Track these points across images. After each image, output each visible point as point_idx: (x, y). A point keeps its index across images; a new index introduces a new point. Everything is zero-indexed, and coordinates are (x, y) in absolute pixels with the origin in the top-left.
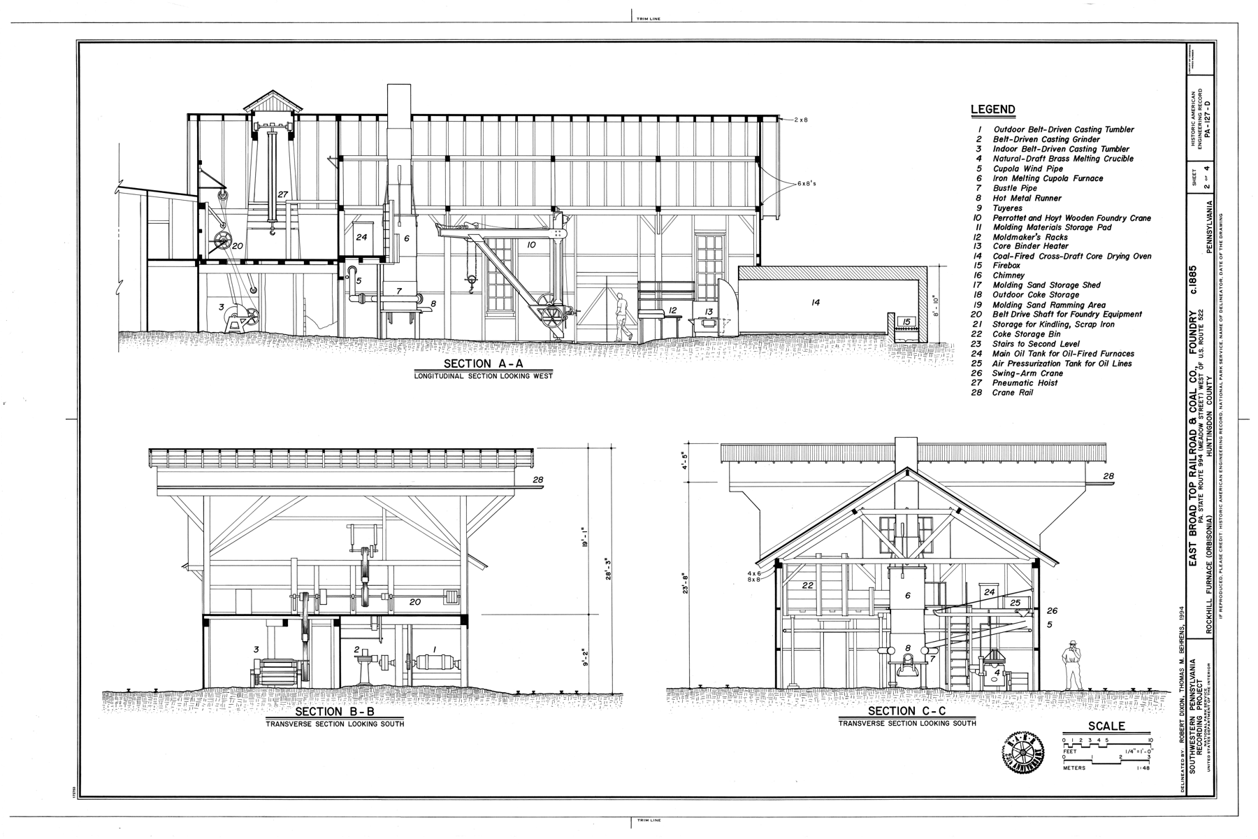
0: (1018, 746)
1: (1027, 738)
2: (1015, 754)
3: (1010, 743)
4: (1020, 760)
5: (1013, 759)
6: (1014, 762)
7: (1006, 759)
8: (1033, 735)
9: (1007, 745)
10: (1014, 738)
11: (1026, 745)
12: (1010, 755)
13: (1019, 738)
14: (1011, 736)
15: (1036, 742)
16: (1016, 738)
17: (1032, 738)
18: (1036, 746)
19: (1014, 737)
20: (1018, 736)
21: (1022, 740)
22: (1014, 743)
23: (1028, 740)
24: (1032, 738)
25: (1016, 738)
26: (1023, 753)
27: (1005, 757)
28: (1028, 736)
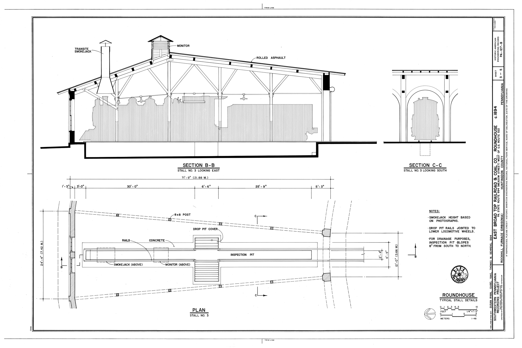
0: (458, 272)
1: (461, 268)
2: (456, 275)
3: (454, 270)
4: (458, 277)
5: (455, 277)
6: (456, 278)
7: (453, 277)
8: (464, 267)
9: (453, 271)
10: (456, 268)
11: (461, 272)
12: (454, 275)
13: (458, 268)
14: (455, 267)
15: (465, 270)
16: (457, 268)
17: (463, 268)
18: (465, 271)
19: (456, 268)
20: (458, 268)
21: (459, 269)
22: (456, 270)
23: (462, 269)
24: (463, 268)
25: (457, 268)
26: (459, 274)
27: (452, 276)
28: (462, 268)
